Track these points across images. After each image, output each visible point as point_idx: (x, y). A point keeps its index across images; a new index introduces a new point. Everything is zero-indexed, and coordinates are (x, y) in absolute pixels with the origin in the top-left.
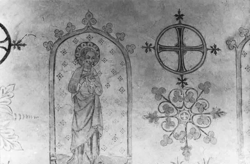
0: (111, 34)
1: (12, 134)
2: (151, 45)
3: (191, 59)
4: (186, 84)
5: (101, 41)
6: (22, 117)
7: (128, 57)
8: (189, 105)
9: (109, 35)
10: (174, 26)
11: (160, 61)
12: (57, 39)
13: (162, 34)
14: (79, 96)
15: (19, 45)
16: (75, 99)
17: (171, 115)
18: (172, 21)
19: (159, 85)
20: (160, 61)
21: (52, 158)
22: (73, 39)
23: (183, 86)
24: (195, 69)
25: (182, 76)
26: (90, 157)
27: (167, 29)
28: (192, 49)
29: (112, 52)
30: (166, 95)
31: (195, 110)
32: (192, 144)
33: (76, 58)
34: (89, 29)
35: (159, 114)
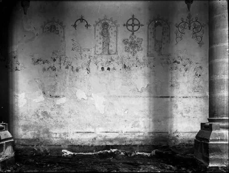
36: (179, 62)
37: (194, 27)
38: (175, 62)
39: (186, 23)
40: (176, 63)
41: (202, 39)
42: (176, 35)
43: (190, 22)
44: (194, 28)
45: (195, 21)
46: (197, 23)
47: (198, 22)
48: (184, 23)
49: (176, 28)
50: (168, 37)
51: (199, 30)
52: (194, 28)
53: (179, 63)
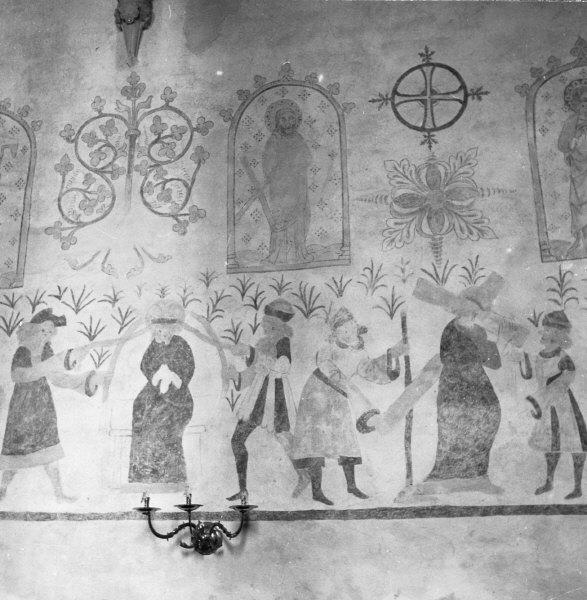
6: (492, 191)
12: (534, 79)
14: (575, 155)
15: (478, 94)
21: (544, 247)
33: (567, 102)
36: (63, 318)
37: (154, 138)
38: (46, 315)
39: (116, 120)
40: (47, 325)
41: (189, 194)
42: (60, 178)
43: (135, 112)
44: (156, 142)
45: (162, 108)
46: (171, 121)
47: (172, 109)
48: (103, 121)
49: (62, 146)
50: (22, 191)
51: (178, 150)
52: (156, 142)
53: (60, 322)
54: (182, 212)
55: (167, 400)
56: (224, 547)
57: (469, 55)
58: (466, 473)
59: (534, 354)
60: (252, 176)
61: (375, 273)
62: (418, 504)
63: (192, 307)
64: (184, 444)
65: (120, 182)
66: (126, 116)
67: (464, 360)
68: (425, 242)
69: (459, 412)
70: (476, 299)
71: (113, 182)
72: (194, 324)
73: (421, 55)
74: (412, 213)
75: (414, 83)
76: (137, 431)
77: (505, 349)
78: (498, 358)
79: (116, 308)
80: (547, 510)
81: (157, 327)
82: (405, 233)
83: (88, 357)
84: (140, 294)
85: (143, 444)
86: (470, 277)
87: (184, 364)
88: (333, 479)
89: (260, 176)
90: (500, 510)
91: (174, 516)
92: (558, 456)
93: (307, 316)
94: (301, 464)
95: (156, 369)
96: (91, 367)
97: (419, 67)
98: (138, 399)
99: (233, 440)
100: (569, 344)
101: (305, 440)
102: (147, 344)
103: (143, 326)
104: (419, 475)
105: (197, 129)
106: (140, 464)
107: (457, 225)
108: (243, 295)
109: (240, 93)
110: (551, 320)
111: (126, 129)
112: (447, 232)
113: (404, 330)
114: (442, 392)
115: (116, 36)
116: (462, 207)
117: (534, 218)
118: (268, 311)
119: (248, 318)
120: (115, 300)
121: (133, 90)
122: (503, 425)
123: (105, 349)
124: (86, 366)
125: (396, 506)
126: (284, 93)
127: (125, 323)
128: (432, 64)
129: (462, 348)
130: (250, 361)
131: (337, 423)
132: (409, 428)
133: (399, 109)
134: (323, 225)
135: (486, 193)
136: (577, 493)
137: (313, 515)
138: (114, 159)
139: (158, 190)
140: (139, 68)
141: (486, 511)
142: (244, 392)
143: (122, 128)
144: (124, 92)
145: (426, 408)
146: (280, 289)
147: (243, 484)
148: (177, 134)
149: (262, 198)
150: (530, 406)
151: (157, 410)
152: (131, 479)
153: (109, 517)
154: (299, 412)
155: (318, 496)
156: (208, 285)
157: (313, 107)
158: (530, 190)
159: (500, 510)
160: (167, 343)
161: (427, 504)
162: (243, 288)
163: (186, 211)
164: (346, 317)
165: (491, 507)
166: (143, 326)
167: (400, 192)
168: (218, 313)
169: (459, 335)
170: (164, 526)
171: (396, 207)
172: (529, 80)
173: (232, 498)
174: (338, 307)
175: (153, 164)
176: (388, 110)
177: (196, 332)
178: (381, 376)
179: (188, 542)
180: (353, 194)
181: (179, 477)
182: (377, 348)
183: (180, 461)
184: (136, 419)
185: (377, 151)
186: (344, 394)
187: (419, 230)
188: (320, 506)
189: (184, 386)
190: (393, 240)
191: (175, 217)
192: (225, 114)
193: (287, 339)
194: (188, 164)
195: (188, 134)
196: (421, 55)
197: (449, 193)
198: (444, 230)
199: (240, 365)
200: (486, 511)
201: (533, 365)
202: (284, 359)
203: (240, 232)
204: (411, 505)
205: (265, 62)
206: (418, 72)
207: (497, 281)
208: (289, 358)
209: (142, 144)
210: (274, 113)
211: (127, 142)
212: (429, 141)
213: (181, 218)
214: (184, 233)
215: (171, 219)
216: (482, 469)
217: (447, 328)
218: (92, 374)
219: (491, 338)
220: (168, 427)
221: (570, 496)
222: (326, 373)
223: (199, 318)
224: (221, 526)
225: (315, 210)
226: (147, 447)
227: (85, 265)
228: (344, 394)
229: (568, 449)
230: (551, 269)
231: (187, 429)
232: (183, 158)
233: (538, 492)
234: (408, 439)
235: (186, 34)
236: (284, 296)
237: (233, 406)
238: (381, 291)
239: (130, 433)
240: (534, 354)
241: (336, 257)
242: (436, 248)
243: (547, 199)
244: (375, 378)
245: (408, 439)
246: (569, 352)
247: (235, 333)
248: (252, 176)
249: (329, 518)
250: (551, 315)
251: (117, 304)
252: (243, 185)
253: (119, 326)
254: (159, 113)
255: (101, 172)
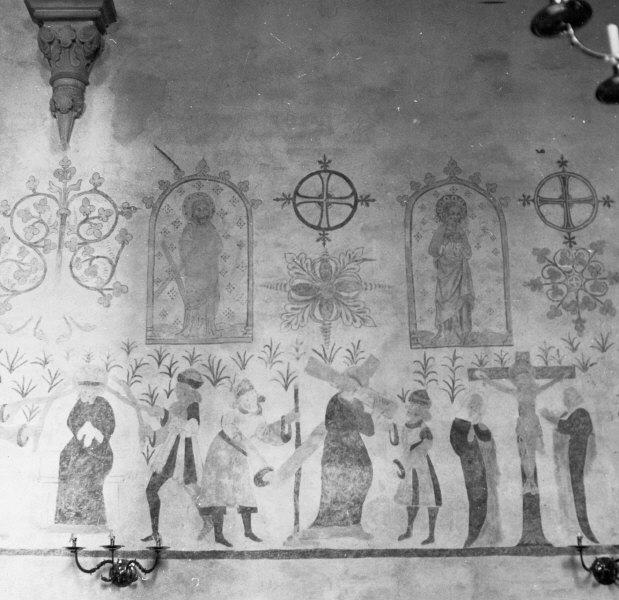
0: (480, 185)
1: (362, 306)
2: (529, 197)
3: (579, 213)
4: (575, 243)
5: (467, 194)
7: (502, 211)
8: (579, 268)
9: (478, 187)
10: (557, 174)
11: (542, 217)
13: (542, 184)
14: (442, 260)
15: (367, 200)
16: (437, 264)
17: (558, 281)
18: (555, 168)
19: (541, 246)
20: (542, 217)
22: (433, 192)
23: (571, 246)
24: (585, 224)
25: (569, 234)
26: (460, 333)
27: (549, 177)
28: (579, 201)
29: (481, 206)
30: (550, 257)
31: (587, 274)
32: (586, 317)
34: (453, 180)
35: (543, 281)
37: (83, 218)
39: (48, 199)
43: (66, 193)
44: (84, 221)
46: (99, 204)
48: (37, 199)
51: (105, 231)
52: (84, 221)
54: (107, 287)
55: (90, 453)
56: (138, 582)
57: (361, 167)
58: (343, 522)
59: (401, 425)
60: (169, 258)
61: (274, 349)
62: (302, 547)
63: (114, 372)
64: (104, 492)
65: (51, 256)
66: (58, 197)
67: (345, 428)
68: (317, 326)
69: (339, 471)
70: (357, 378)
71: (46, 256)
72: (116, 387)
73: (320, 162)
74: (308, 301)
75: (313, 187)
76: (63, 479)
77: (378, 420)
78: (372, 426)
79: (46, 370)
80: (408, 553)
81: (84, 389)
82: (300, 319)
83: (20, 412)
84: (67, 358)
85: (68, 492)
86: (353, 359)
87: (105, 419)
88: (233, 525)
89: (177, 261)
90: (370, 553)
91: (96, 554)
92: (417, 509)
93: (214, 384)
94: (205, 512)
95: (81, 425)
96: (24, 421)
97: (318, 173)
98: (64, 451)
99: (148, 489)
100: (429, 417)
101: (210, 492)
102: (73, 403)
103: (70, 387)
104: (306, 521)
105: (122, 213)
106: (65, 508)
107: (343, 314)
108: (159, 363)
109: (162, 183)
110: (416, 397)
111: (57, 208)
112: (336, 319)
113: (296, 401)
114: (326, 454)
115: (50, 121)
116: (348, 298)
117: (406, 311)
118: (181, 378)
119: (163, 384)
120: (46, 363)
121: (64, 173)
122: (375, 483)
123: (36, 405)
124: (17, 420)
125: (284, 548)
126: (200, 186)
127: (55, 382)
128: (329, 171)
129: (344, 418)
130: (164, 422)
131: (237, 477)
132: (297, 484)
133: (299, 209)
134: (231, 305)
135: (369, 288)
136: (431, 539)
137: (215, 555)
138: (46, 235)
139: (86, 266)
140: (70, 154)
141: (358, 554)
142: (157, 448)
143: (54, 207)
144: (57, 173)
145: (313, 465)
146: (192, 360)
147: (155, 528)
148: (103, 216)
149: (178, 280)
150: (396, 468)
151: (82, 461)
152: (57, 521)
153: (38, 552)
154: (205, 468)
155: (220, 539)
156: (128, 353)
157: (224, 200)
158: (404, 288)
159: (370, 553)
160: (91, 403)
161: (311, 547)
162: (160, 356)
163: (110, 286)
164: (248, 387)
165: (362, 551)
166: (70, 387)
167: (298, 282)
168: (136, 378)
169: (342, 406)
170: (88, 562)
171: (293, 295)
172: (409, 192)
173: (147, 539)
174: (241, 378)
175: (82, 241)
176: (290, 208)
177: (117, 394)
178: (275, 439)
179: (106, 575)
180: (258, 281)
181: (99, 520)
182: (273, 415)
183: (101, 506)
184: (62, 469)
185: (279, 245)
186: (245, 453)
187: (312, 315)
188: (220, 547)
189: (106, 441)
190: (289, 323)
191: (100, 291)
192: (147, 201)
193: (197, 404)
194: (113, 244)
195: (114, 216)
196: (320, 162)
197: (339, 284)
198: (332, 318)
199: (156, 425)
200: (358, 554)
201: (400, 435)
202: (193, 421)
203: (159, 308)
204: (299, 548)
205: (187, 157)
206: (317, 176)
207: (373, 361)
208: (198, 420)
209: (72, 223)
210: (190, 205)
211: (59, 220)
212: (323, 239)
213: (105, 292)
214: (108, 306)
215: (96, 293)
216: (357, 519)
217: (332, 400)
218: (24, 426)
219: (368, 410)
220: (91, 477)
221: (424, 543)
222: (229, 434)
223: (120, 382)
224: (137, 564)
225: (224, 292)
226: (72, 493)
227: (18, 330)
228: (245, 453)
229: (425, 504)
230: (418, 355)
231: (108, 478)
232: (108, 238)
233: (400, 538)
234: (297, 493)
235: (114, 125)
236: (195, 366)
237: (148, 460)
238: (277, 367)
239: (57, 480)
240: (401, 425)
241: (241, 334)
242: (325, 331)
243: (417, 295)
244: (270, 440)
245: (297, 493)
246: (428, 424)
247: (152, 397)
248: (169, 258)
249: (229, 558)
250: (416, 393)
251: (48, 366)
252: (162, 264)
253: (48, 387)
254: (88, 196)
255: (34, 245)
